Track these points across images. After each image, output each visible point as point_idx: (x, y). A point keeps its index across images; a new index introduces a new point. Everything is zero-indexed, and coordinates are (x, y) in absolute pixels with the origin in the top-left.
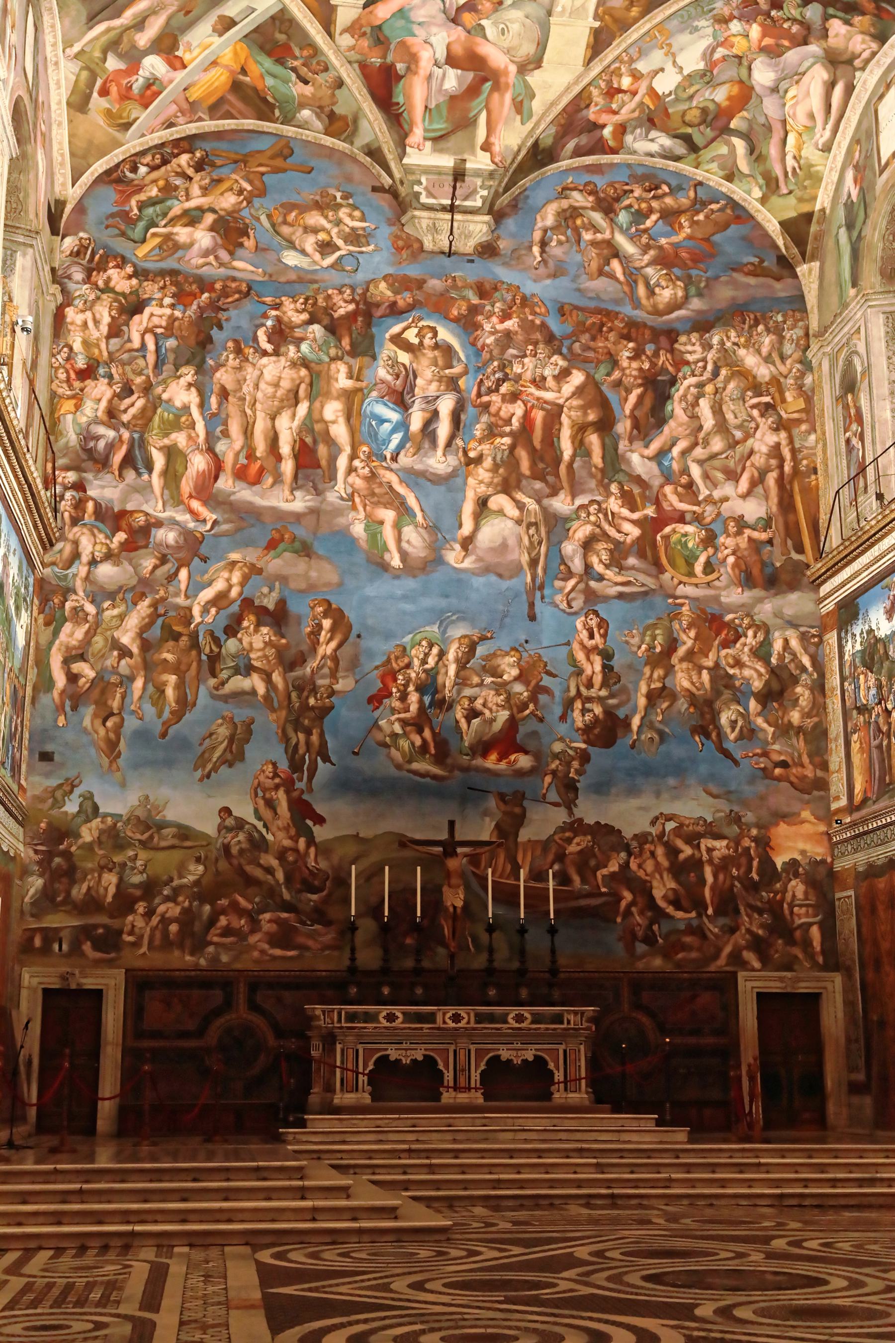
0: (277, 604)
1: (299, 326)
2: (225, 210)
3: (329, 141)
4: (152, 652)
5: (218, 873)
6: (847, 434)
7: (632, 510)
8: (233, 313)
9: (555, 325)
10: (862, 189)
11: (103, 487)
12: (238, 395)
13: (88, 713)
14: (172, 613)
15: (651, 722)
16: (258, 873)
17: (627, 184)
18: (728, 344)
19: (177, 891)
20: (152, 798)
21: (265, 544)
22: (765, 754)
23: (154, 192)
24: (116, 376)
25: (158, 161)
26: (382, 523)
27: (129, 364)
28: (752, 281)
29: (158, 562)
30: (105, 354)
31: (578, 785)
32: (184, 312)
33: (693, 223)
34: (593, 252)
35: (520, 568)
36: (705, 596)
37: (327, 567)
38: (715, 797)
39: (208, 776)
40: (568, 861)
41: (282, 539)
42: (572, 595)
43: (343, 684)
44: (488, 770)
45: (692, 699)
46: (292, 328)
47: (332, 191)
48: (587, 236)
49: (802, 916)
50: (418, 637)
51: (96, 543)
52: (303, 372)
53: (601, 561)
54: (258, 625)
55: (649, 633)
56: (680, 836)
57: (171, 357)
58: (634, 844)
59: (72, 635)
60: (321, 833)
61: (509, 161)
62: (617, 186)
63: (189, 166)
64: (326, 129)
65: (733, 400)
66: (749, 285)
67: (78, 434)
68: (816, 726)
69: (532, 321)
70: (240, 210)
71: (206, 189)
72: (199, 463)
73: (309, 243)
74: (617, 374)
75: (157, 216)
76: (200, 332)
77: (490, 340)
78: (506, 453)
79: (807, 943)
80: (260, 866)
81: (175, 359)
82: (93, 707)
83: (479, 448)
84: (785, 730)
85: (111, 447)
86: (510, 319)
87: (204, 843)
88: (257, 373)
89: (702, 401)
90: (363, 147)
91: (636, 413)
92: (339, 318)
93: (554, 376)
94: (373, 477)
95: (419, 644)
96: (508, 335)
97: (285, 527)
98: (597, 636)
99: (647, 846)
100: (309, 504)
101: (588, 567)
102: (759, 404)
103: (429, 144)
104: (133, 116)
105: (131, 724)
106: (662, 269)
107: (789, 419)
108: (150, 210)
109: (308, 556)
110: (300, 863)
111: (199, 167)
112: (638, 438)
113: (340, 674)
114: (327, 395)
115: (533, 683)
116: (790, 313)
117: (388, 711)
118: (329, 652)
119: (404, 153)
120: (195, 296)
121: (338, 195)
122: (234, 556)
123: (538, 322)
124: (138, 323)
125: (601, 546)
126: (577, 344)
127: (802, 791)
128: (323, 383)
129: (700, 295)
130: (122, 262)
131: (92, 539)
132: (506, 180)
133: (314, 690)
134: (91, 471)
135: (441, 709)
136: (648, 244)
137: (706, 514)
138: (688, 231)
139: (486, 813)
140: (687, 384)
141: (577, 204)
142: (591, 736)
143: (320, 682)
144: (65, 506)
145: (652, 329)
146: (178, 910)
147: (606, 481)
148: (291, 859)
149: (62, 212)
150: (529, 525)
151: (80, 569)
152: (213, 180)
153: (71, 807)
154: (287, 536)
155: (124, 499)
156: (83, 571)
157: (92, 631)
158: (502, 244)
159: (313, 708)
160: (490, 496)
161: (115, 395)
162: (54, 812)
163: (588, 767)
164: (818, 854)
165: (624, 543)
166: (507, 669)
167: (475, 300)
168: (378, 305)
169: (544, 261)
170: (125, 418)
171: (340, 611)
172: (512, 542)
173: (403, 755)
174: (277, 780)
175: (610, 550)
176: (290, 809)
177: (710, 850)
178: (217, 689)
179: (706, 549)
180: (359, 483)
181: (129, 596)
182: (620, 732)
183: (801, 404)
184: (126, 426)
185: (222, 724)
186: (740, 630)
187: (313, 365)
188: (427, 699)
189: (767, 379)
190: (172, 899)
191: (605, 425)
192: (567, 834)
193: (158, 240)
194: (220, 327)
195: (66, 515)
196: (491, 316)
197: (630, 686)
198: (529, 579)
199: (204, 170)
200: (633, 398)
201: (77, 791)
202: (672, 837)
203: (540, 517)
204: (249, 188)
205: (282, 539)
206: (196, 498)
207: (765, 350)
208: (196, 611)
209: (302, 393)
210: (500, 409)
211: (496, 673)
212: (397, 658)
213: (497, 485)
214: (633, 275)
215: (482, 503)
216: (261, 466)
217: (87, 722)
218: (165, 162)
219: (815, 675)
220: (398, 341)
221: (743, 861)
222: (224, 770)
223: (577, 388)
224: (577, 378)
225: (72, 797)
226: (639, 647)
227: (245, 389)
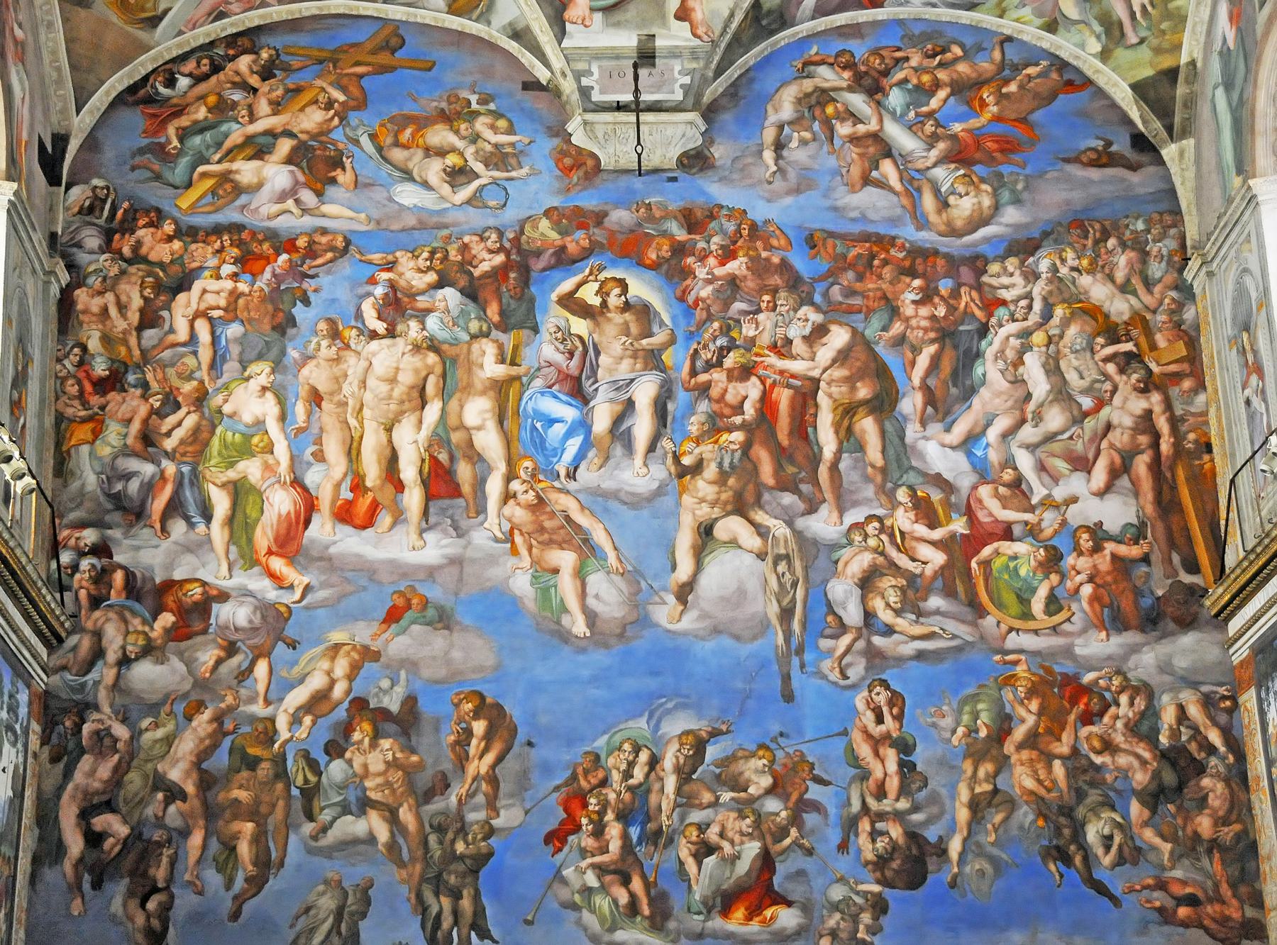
0: (403, 704)
1: (423, 293)
2: (307, 132)
3: (455, 23)
4: (214, 791)
6: (1247, 392)
7: (932, 526)
8: (324, 280)
9: (801, 263)
10: (1239, 30)
11: (138, 548)
12: (336, 399)
13: (117, 893)
14: (246, 729)
17: (899, 49)
18: (1064, 271)
21: (384, 615)
23: (201, 113)
24: (155, 386)
25: (205, 68)
26: (556, 571)
27: (173, 365)
28: (1095, 174)
29: (222, 654)
30: (137, 353)
33: (1001, 98)
34: (853, 152)
35: (765, 625)
37: (479, 643)
41: (409, 607)
42: (847, 659)
46: (413, 296)
47: (464, 94)
48: (843, 129)
51: (127, 633)
52: (432, 358)
53: (888, 605)
54: (376, 736)
57: (235, 350)
59: (92, 773)
61: (718, 30)
62: (883, 53)
63: (252, 72)
64: (450, 6)
65: (1077, 351)
66: (1091, 182)
67: (98, 474)
70: (330, 131)
71: (279, 104)
72: (281, 502)
73: (434, 170)
74: (897, 328)
75: (208, 147)
76: (277, 310)
77: (706, 292)
78: (738, 455)
81: (241, 353)
82: (126, 881)
83: (697, 451)
85: (150, 488)
86: (735, 258)
88: (364, 364)
89: (1028, 357)
90: (504, 28)
91: (932, 382)
92: (481, 277)
93: (804, 337)
94: (540, 504)
95: (619, 749)
97: (412, 588)
100: (449, 551)
101: (869, 615)
103: (598, 16)
104: (162, 7)
105: (185, 902)
106: (957, 169)
107: (1165, 375)
108: (197, 140)
109: (448, 628)
112: (934, 419)
113: (501, 803)
114: (468, 389)
115: (794, 797)
117: (576, 854)
118: (483, 770)
120: (268, 260)
121: (474, 99)
122: (337, 636)
123: (776, 260)
124: (183, 307)
126: (836, 288)
128: (461, 373)
129: (1017, 201)
130: (157, 217)
131: (123, 626)
132: (717, 58)
133: (462, 831)
134: (118, 526)
135: (656, 845)
137: (1044, 525)
138: (995, 109)
140: (1004, 333)
141: (826, 85)
143: (472, 817)
144: (82, 578)
145: (948, 257)
149: (64, 151)
150: (777, 559)
151: (105, 673)
152: (288, 91)
154: (415, 601)
156: (109, 675)
157: (124, 765)
158: (719, 152)
159: (462, 858)
160: (716, 520)
161: (153, 412)
165: (921, 575)
166: (754, 778)
167: (681, 235)
168: (538, 254)
169: (780, 170)
170: (169, 444)
171: (499, 707)
172: (753, 585)
173: (602, 920)
175: (901, 588)
178: (315, 838)
180: (518, 513)
181: (180, 708)
184: (170, 456)
185: (324, 893)
187: (445, 347)
188: (634, 832)
189: (1126, 317)
193: (209, 183)
194: (306, 302)
195: (83, 593)
196: (706, 257)
198: (780, 639)
199: (275, 76)
200: (923, 361)
203: (793, 545)
204: (342, 98)
205: (409, 607)
207: (1120, 276)
208: (282, 723)
209: (430, 389)
210: (726, 391)
211: (738, 785)
212: (586, 772)
213: (726, 503)
214: (913, 181)
215: (706, 531)
217: (117, 906)
218: (216, 69)
220: (570, 302)
223: (840, 352)
224: (839, 337)
227: (349, 388)
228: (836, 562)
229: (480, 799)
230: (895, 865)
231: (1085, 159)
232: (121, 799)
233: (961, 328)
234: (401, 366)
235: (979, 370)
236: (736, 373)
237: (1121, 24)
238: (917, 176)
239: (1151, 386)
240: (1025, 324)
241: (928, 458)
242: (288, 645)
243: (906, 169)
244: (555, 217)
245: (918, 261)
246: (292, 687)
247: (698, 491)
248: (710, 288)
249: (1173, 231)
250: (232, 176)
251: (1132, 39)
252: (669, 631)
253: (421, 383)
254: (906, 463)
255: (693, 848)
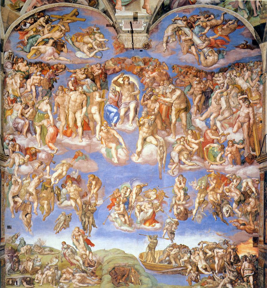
1: (82, 80)
3: (91, 8)
5: (62, 262)
7: (196, 140)
11: (21, 140)
12: (63, 106)
15: (199, 212)
16: (74, 261)
18: (233, 76)
19: (50, 267)
20: (42, 240)
22: (238, 221)
23: (32, 33)
24: (23, 101)
26: (111, 148)
27: (27, 97)
28: (243, 51)
30: (19, 94)
31: (175, 233)
32: (44, 77)
33: (223, 29)
34: (185, 44)
36: (220, 169)
37: (94, 164)
38: (220, 235)
39: (58, 232)
40: (171, 257)
41: (79, 155)
42: (174, 170)
43: (100, 202)
44: (145, 229)
45: (213, 203)
47: (93, 28)
48: (183, 38)
49: (247, 273)
50: (123, 186)
52: (84, 96)
54: (72, 183)
55: (200, 182)
56: (208, 249)
57: (41, 93)
58: (193, 251)
60: (93, 249)
68: (256, 211)
69: (163, 72)
72: (51, 130)
73: (85, 48)
74: (192, 90)
77: (148, 81)
78: (153, 121)
79: (248, 281)
80: (75, 259)
83: (144, 120)
84: (246, 214)
85: (23, 126)
87: (58, 253)
89: (222, 99)
91: (198, 104)
93: (170, 92)
94: (108, 132)
96: (154, 78)
98: (182, 183)
99: (197, 252)
100: (87, 143)
101: (180, 160)
102: (242, 98)
103: (124, 7)
105: (34, 217)
107: (253, 103)
108: (31, 40)
109: (87, 160)
110: (87, 258)
111: (47, 22)
113: (98, 199)
114: (92, 104)
115: (161, 200)
116: (256, 62)
119: (115, 12)
121: (95, 29)
122: (64, 161)
123: (165, 72)
124: (30, 82)
125: (184, 153)
126: (178, 80)
127: (249, 233)
128: (91, 100)
129: (223, 58)
130: (23, 60)
133: (90, 204)
134: (17, 135)
136: (205, 39)
139: (145, 242)
141: (180, 26)
142: (179, 217)
143: (92, 202)
146: (51, 273)
147: (187, 130)
148: (84, 257)
150: (160, 146)
152: (52, 27)
153: (17, 242)
155: (28, 145)
156: (16, 168)
157: (20, 188)
158: (153, 44)
159: (90, 210)
160: (147, 137)
162: (13, 244)
163: (178, 227)
164: (253, 253)
166: (152, 196)
167: (143, 66)
168: (109, 70)
170: (27, 116)
171: (98, 179)
172: (154, 153)
173: (119, 225)
174: (80, 233)
175: (187, 154)
176: (84, 242)
177: (217, 253)
179: (221, 152)
181: (31, 176)
182: (189, 215)
183: (258, 97)
185: (62, 216)
186: (231, 180)
187: (87, 94)
188: (126, 206)
189: (246, 89)
190: (49, 269)
191: (187, 109)
192: (171, 248)
193: (34, 51)
194: (56, 82)
195: (10, 150)
197: (193, 200)
199: (49, 23)
200: (197, 99)
201: (19, 238)
202: (205, 249)
204: (64, 29)
205: (79, 155)
206: (51, 142)
207: (246, 78)
209: (84, 104)
212: (116, 193)
215: (145, 140)
216: (71, 130)
219: (257, 194)
220: (116, 83)
221: (228, 256)
222: (63, 230)
224: (178, 93)
225: (17, 239)
226: (196, 187)
227: (65, 103)
228: (174, 147)
229: (94, 198)
230: (181, 215)
231: (241, 47)
232: (20, 194)
233: (207, 91)
234: (77, 98)
235: (210, 102)
236: (154, 101)
237: (253, 10)
238: (200, 51)
239: (250, 106)
240: (222, 90)
241: (196, 123)
242: (53, 163)
243: (197, 49)
244: (113, 61)
245: (198, 73)
246: (54, 172)
247: (143, 130)
248: (148, 80)
249: (260, 66)
250: (39, 49)
251: (256, 15)
252: (135, 162)
253: (82, 102)
254: (191, 124)
255: (138, 210)
